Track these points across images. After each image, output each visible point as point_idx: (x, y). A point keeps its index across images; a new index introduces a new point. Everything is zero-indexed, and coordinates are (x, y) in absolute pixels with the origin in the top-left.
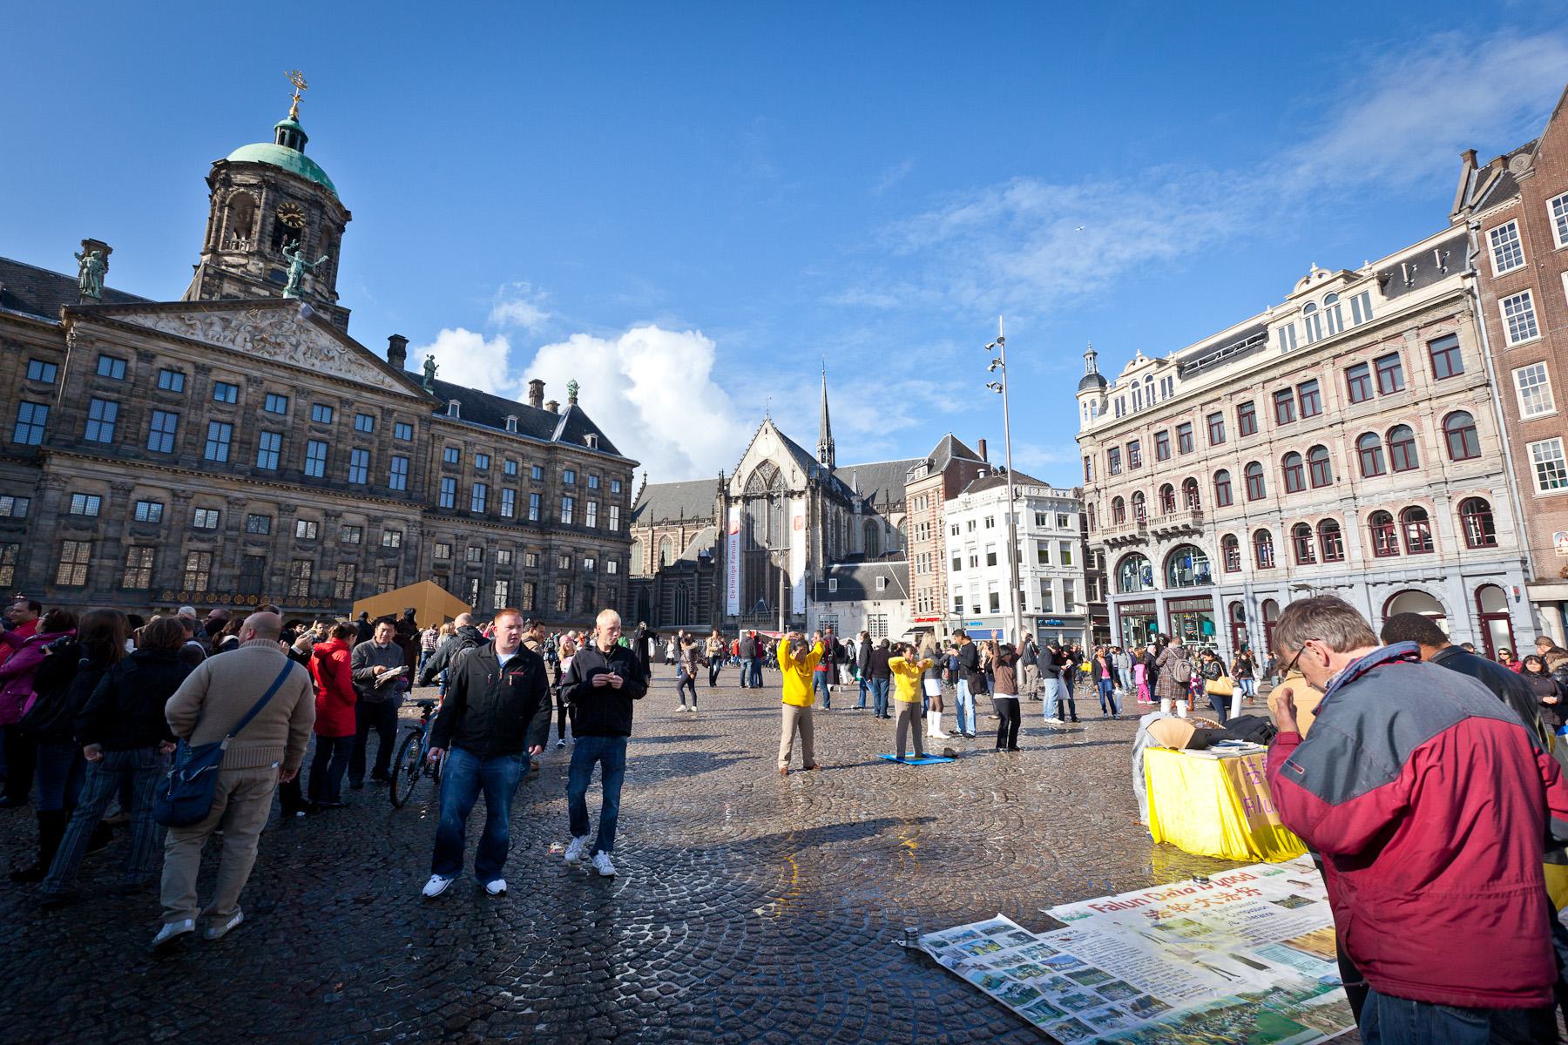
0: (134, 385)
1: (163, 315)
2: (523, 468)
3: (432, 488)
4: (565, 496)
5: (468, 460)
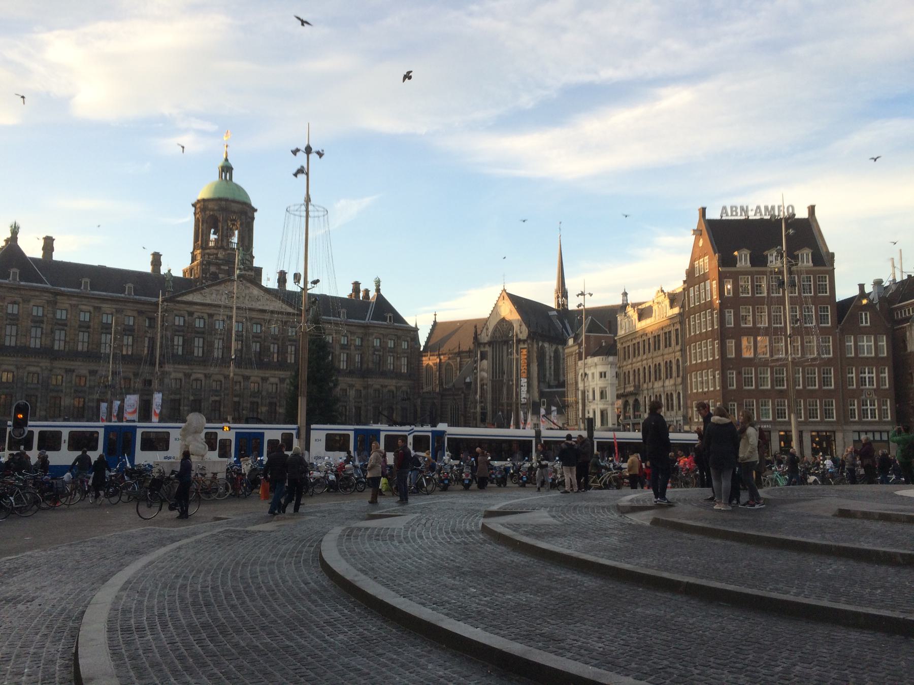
0: (188, 328)
2: (351, 340)
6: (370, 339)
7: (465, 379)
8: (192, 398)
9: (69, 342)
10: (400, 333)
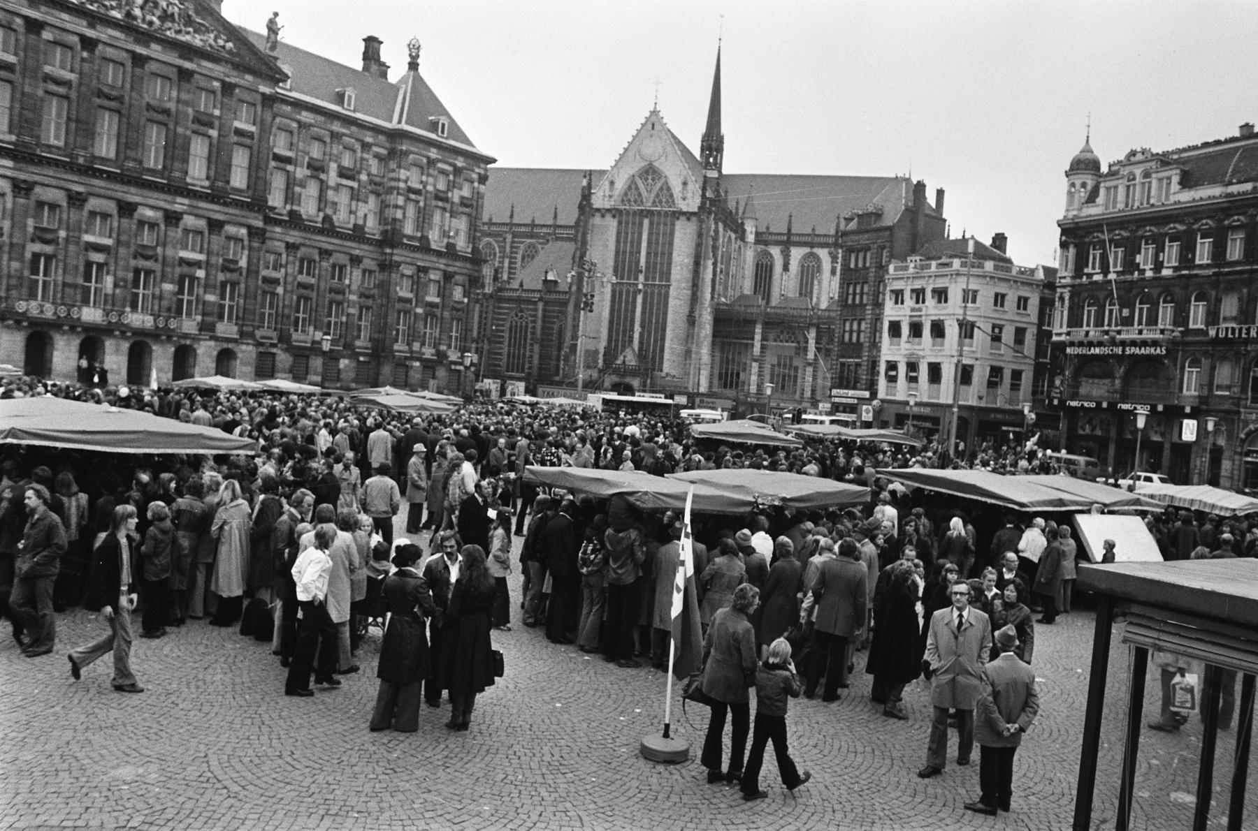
2: (362, 159)
7: (546, 272)
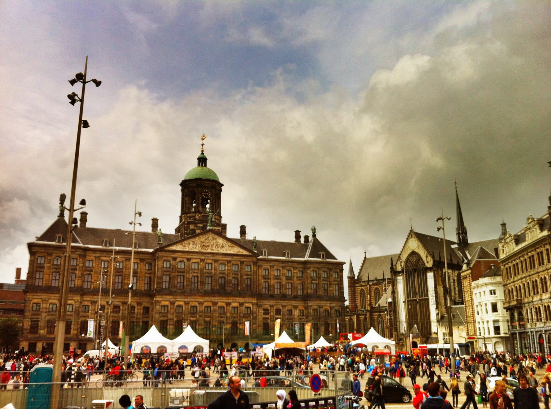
1: (178, 244)
2: (294, 273)
3: (260, 287)
4: (312, 283)
5: (272, 273)
6: (308, 271)
8: (175, 319)
9: (94, 283)
10: (331, 267)
